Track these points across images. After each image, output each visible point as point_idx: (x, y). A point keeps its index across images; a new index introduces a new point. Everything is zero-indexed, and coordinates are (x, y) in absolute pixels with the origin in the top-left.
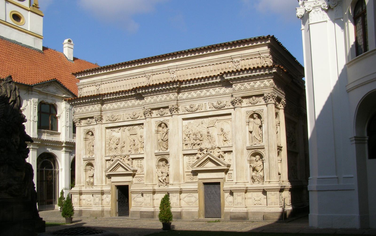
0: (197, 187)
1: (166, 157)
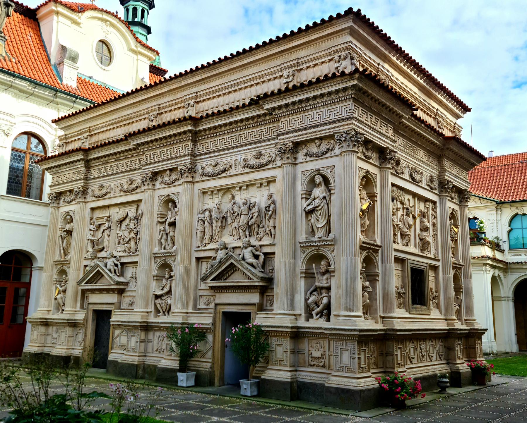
0: (209, 321)
1: (170, 261)
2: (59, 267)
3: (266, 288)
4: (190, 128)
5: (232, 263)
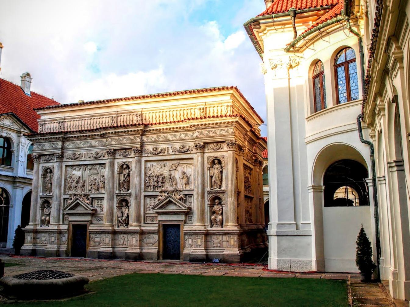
0: (157, 228)
1: (127, 198)
2: (42, 200)
3: (189, 213)
4: (142, 128)
5: (170, 200)
